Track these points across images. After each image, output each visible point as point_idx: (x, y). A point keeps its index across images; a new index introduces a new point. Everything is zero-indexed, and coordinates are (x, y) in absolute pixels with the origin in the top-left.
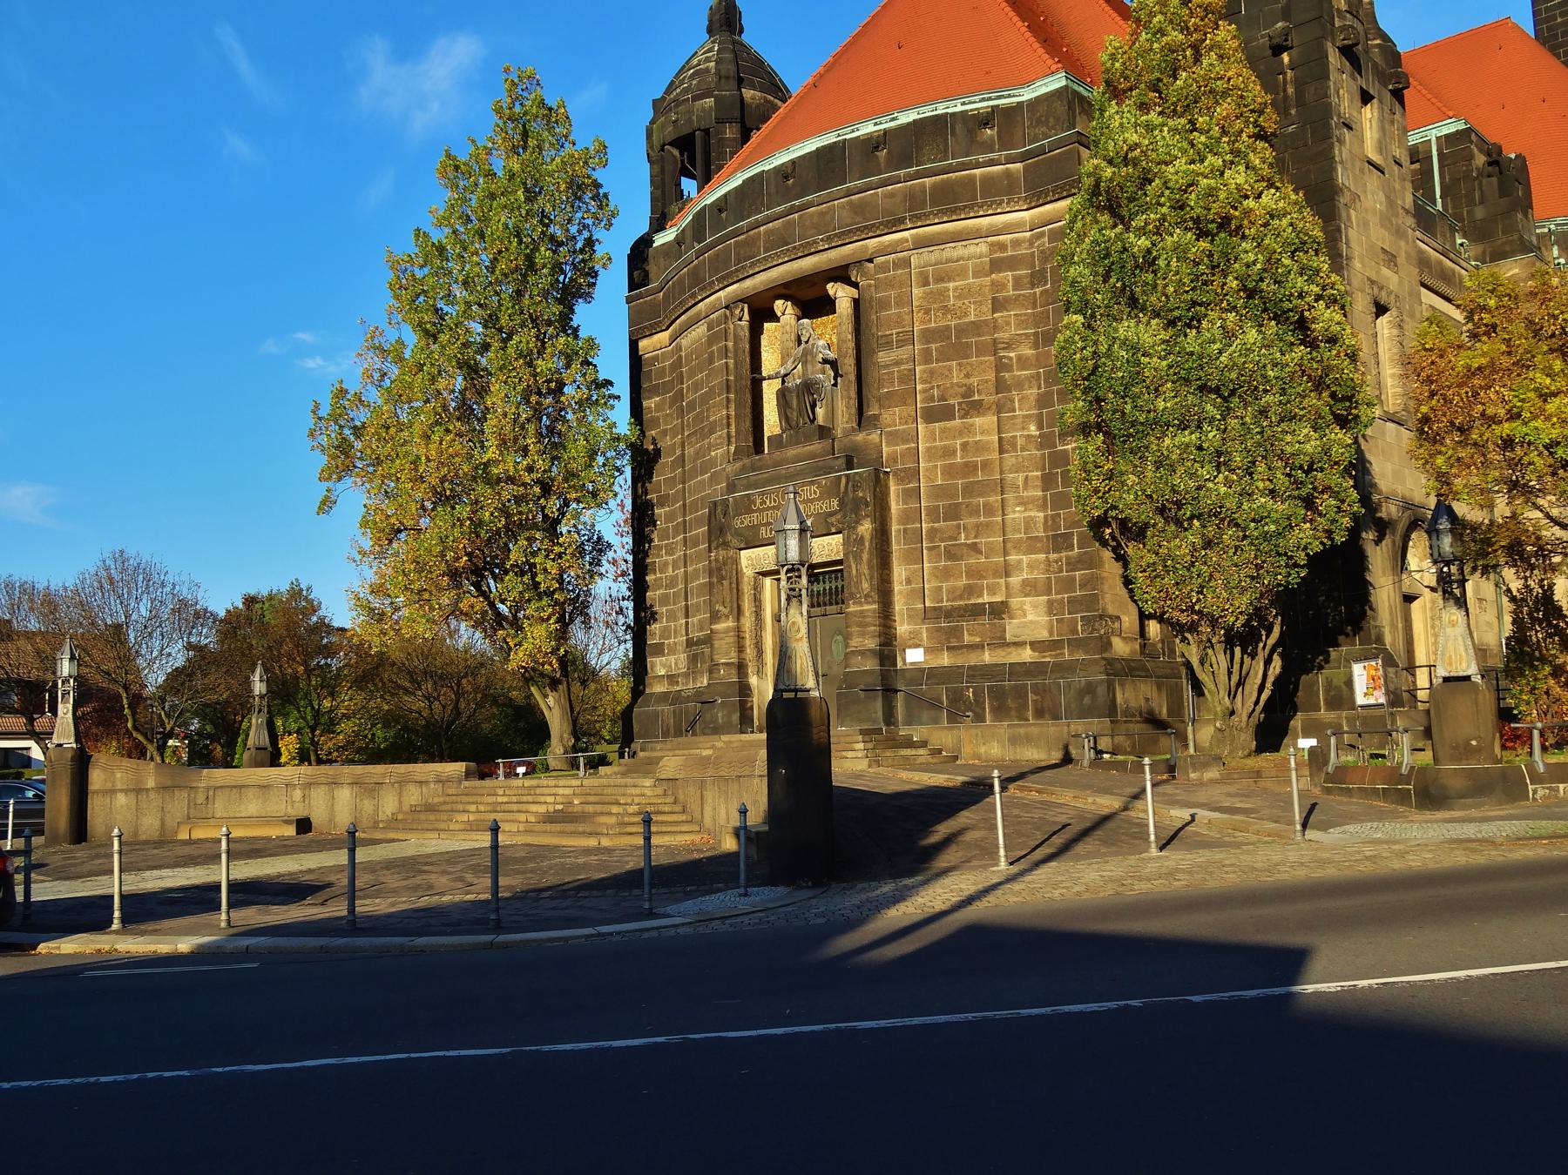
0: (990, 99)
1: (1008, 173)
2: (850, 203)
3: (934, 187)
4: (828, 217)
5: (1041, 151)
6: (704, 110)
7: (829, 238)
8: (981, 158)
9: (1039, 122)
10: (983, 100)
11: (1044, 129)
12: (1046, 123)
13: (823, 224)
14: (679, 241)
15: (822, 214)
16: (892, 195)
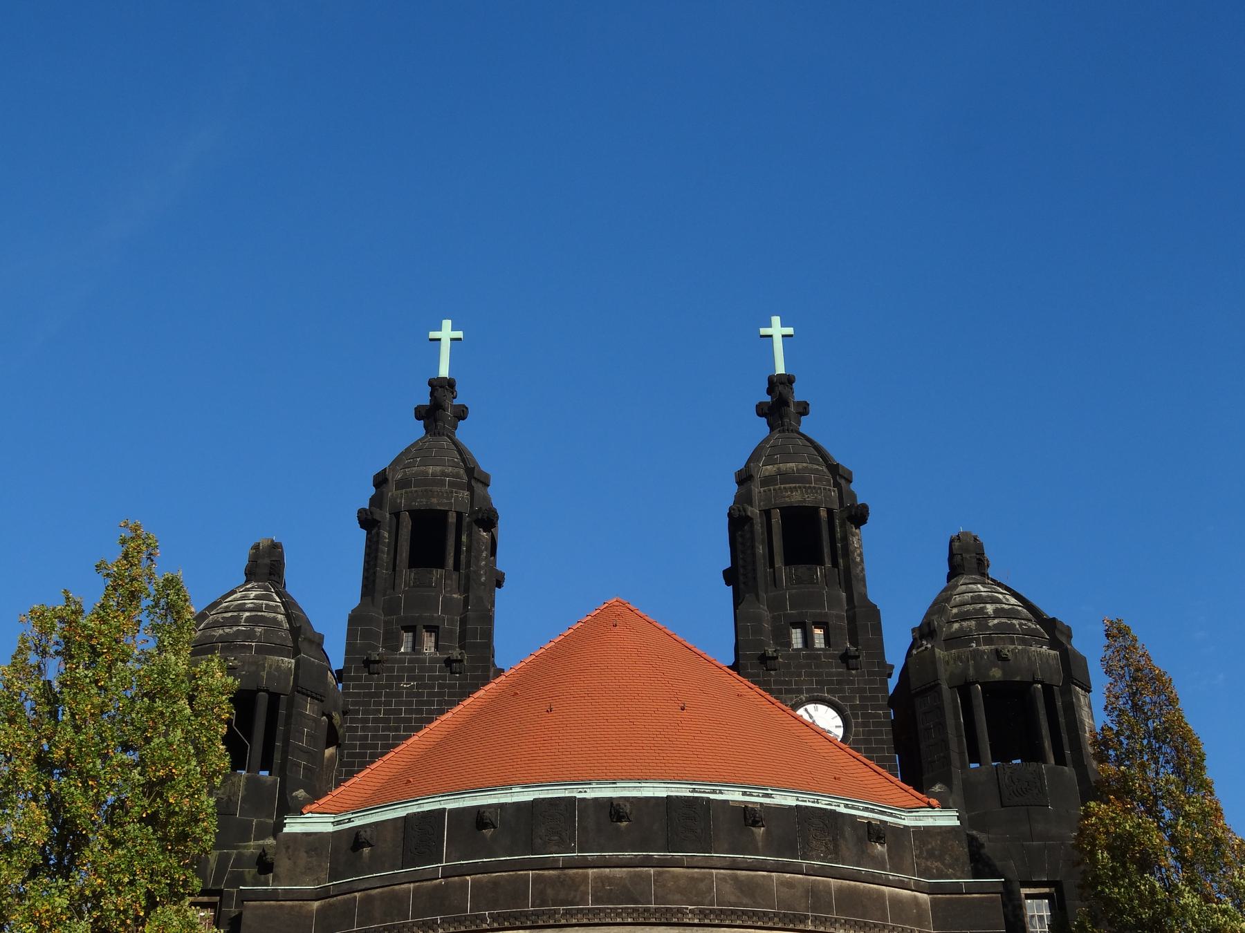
0: (872, 811)
1: (915, 901)
2: (735, 878)
3: (840, 890)
4: (702, 886)
5: (956, 889)
6: (278, 668)
7: (701, 911)
8: (893, 876)
9: (931, 855)
10: (866, 809)
11: (938, 864)
12: (940, 858)
13: (692, 890)
14: (357, 839)
15: (692, 879)
16: (790, 885)
